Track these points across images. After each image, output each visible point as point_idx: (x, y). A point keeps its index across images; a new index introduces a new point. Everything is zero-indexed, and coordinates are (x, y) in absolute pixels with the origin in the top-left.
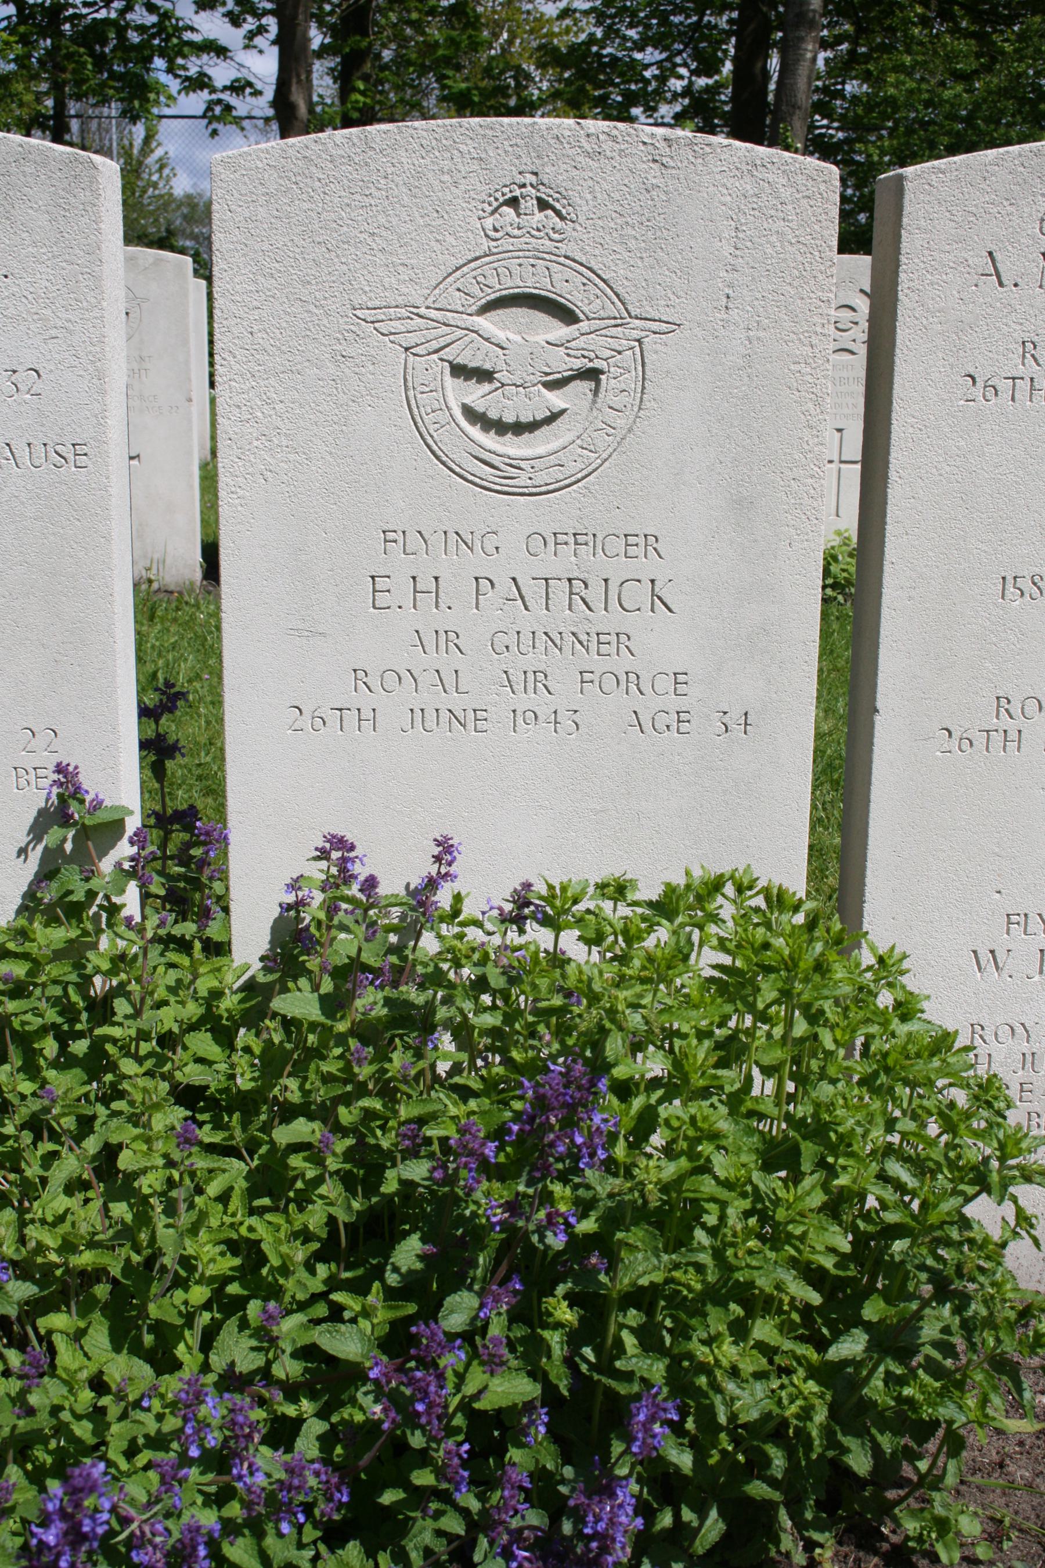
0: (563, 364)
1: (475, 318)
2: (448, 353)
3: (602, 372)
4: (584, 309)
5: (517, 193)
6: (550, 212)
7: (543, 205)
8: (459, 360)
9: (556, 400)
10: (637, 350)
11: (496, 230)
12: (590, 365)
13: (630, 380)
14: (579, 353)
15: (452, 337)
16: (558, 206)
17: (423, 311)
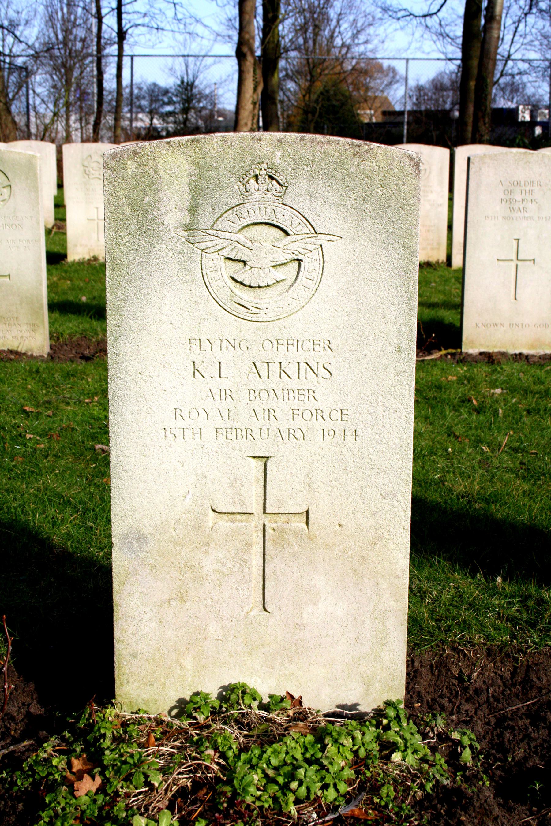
0: (281, 257)
1: (238, 235)
2: (225, 253)
3: (302, 261)
4: (293, 230)
5: (257, 172)
6: (274, 182)
7: (271, 177)
8: (229, 256)
9: (279, 273)
10: (320, 249)
11: (247, 192)
12: (296, 257)
13: (317, 265)
14: (290, 252)
15: (225, 245)
16: (277, 178)
17: (210, 232)
